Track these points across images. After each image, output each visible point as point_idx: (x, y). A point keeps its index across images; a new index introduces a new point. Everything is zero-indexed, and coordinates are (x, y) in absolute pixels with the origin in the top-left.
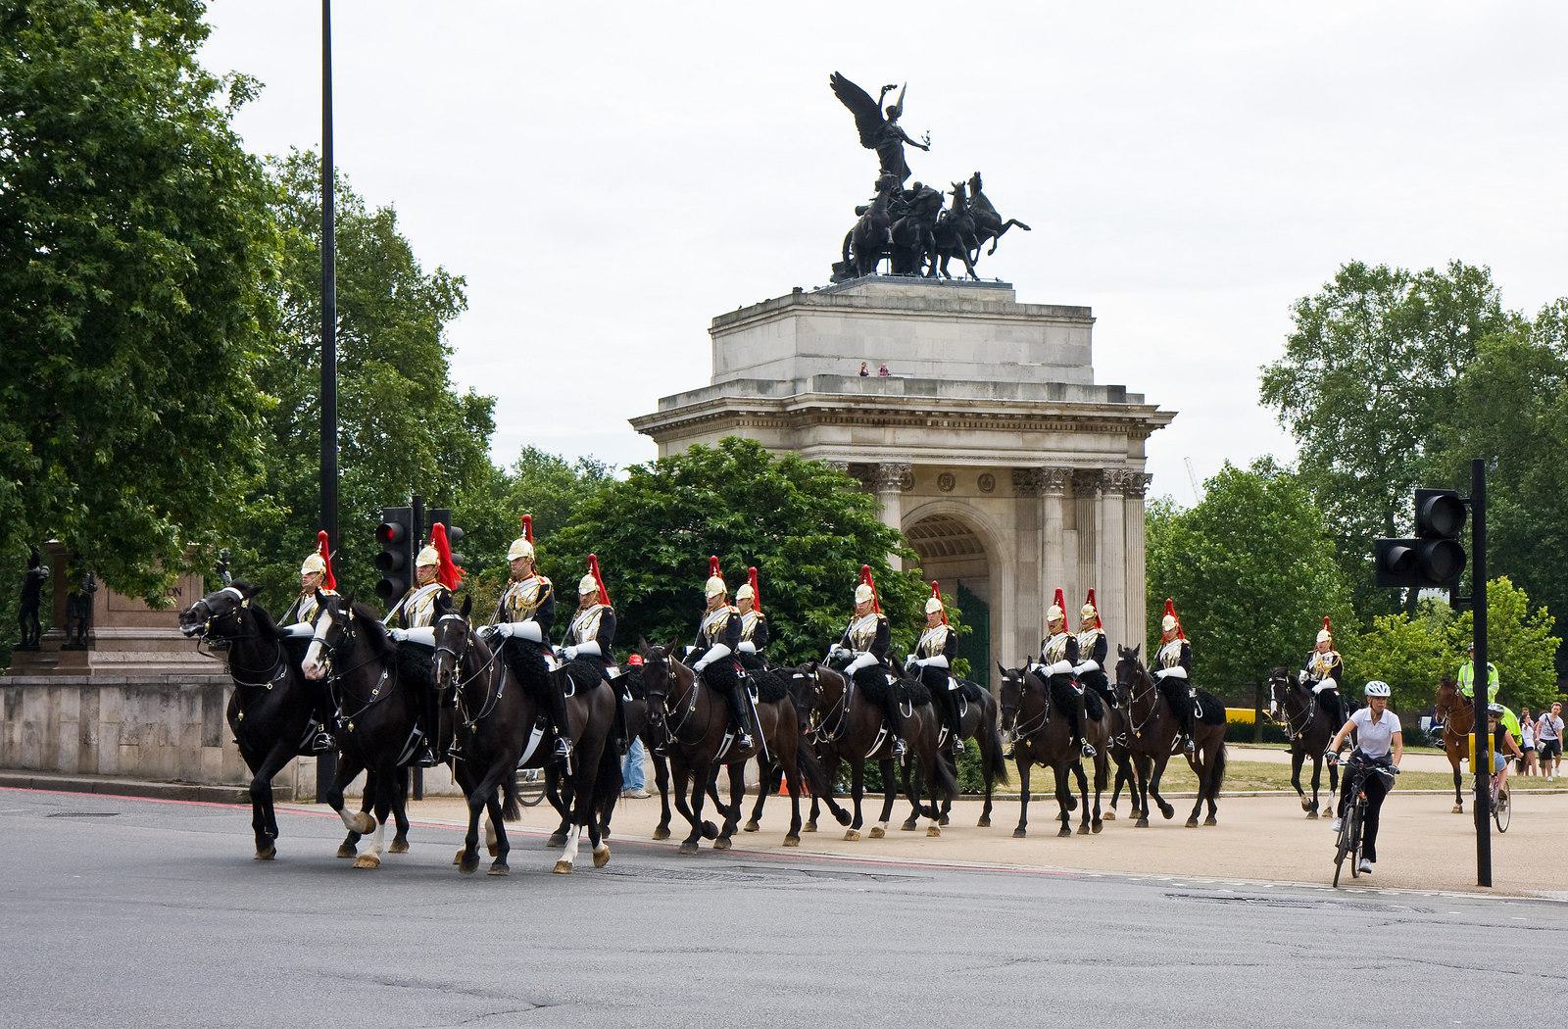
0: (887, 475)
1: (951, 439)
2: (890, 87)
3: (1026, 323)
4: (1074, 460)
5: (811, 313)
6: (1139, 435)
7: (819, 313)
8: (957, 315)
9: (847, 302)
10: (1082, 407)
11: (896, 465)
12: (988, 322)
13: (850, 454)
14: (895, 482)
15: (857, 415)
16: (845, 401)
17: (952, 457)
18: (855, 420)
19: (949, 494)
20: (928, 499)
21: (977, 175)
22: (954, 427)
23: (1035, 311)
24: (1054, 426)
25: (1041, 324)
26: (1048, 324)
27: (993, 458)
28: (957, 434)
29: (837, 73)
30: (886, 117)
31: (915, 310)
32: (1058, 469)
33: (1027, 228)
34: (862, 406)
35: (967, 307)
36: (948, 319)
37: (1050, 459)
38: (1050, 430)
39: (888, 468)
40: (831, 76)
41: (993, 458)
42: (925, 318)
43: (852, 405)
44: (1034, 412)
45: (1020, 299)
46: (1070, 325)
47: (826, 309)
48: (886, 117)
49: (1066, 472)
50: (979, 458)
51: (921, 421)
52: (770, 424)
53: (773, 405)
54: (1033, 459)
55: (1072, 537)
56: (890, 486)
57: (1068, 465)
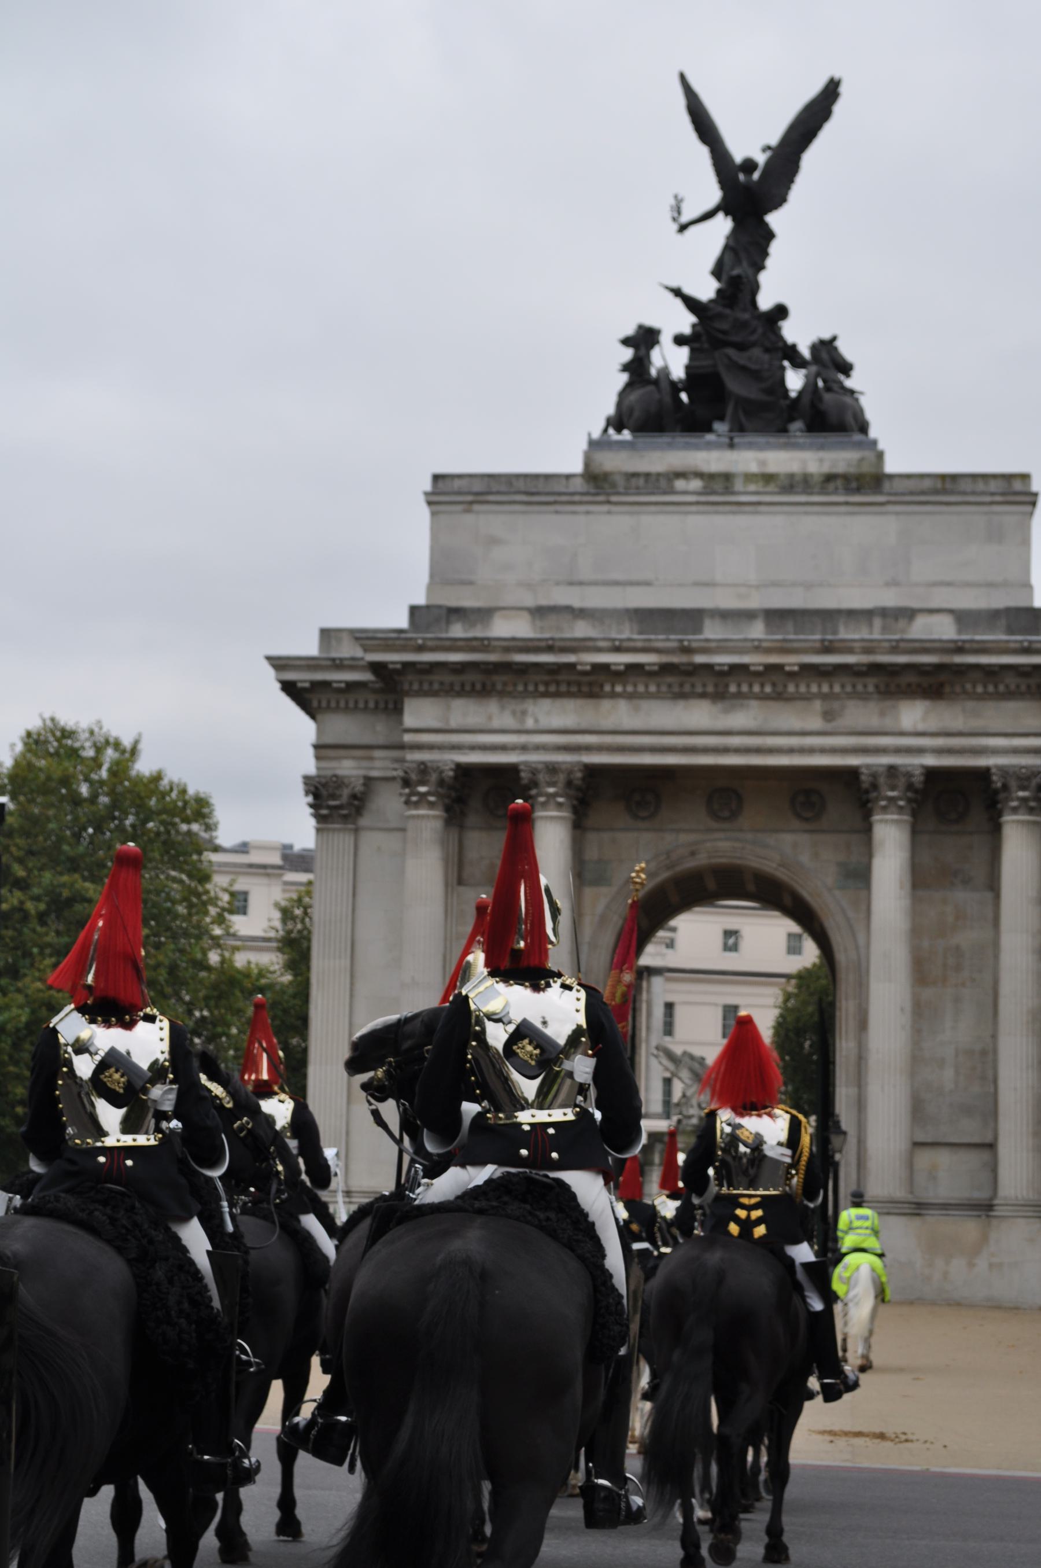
20: (684, 838)
39: (534, 772)
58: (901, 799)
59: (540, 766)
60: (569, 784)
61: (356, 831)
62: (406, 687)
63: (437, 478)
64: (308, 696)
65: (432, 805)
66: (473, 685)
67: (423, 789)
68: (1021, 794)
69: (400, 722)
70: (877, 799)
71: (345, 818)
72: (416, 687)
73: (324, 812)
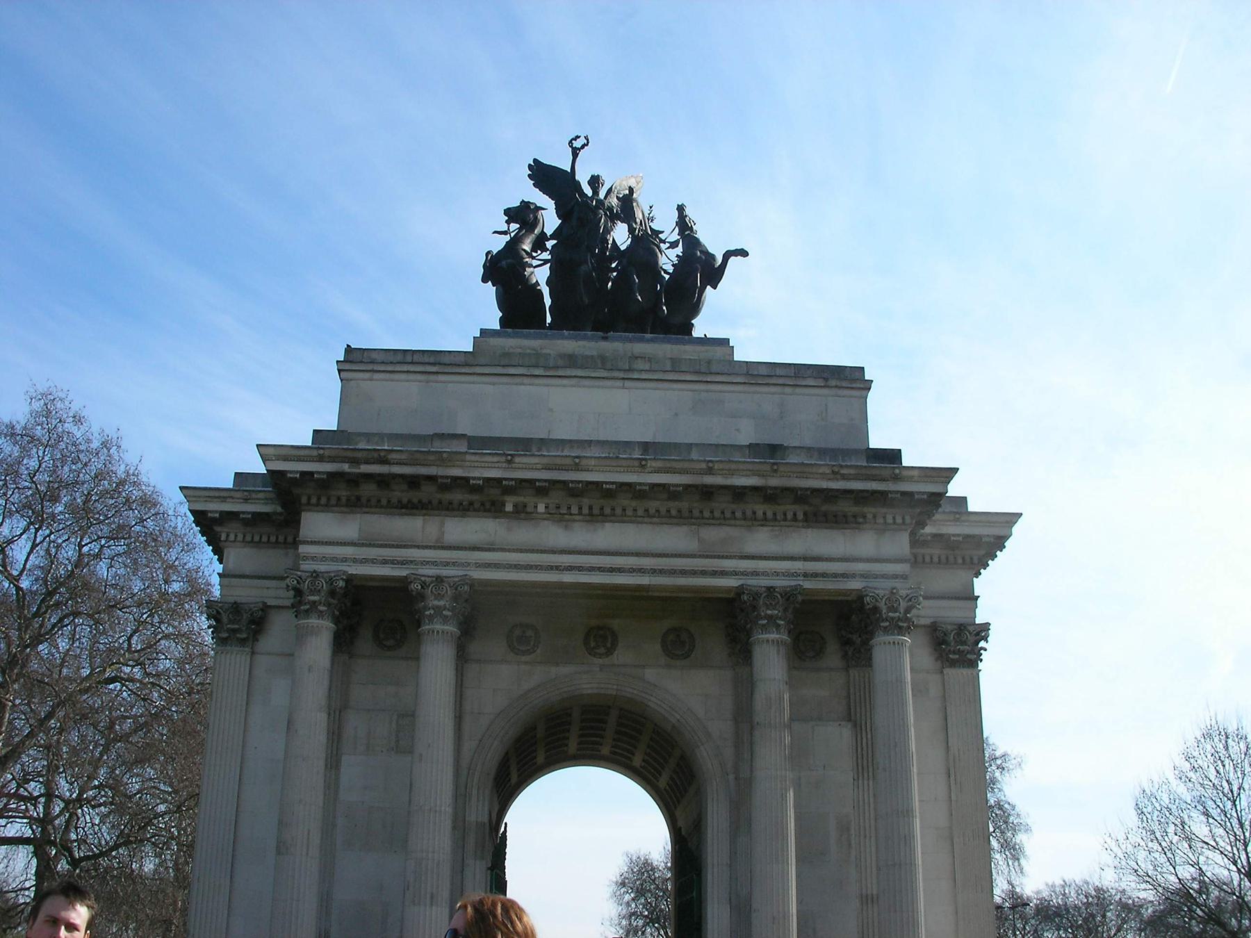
0: (422, 597)
1: (554, 535)
2: (578, 137)
3: (746, 388)
4: (805, 575)
5: (367, 375)
6: (960, 561)
7: (382, 376)
8: (622, 375)
9: (432, 360)
10: (803, 470)
11: (439, 580)
12: (675, 386)
13: (355, 561)
14: (438, 609)
15: (368, 490)
16: (332, 459)
17: (557, 568)
18: (364, 500)
19: (606, 661)
21: (681, 209)
22: (559, 516)
23: (763, 371)
24: (760, 514)
25: (773, 389)
26: (788, 390)
27: (641, 571)
28: (566, 527)
29: (535, 160)
30: (588, 191)
31: (546, 368)
32: (770, 590)
33: (743, 253)
34: (365, 469)
35: (640, 365)
36: (609, 383)
37: (755, 573)
38: (754, 521)
39: (424, 585)
40: (530, 165)
41: (641, 571)
42: (565, 381)
43: (346, 467)
44: (709, 480)
45: (739, 356)
46: (825, 391)
47: (390, 368)
48: (588, 191)
49: (789, 595)
50: (612, 570)
51: (493, 503)
52: (273, 539)
53: (267, 501)
54: (723, 573)
55: (838, 737)
56: (431, 618)
57: (793, 583)
58: (780, 619)
59: (428, 580)
60: (455, 598)
61: (253, 653)
62: (304, 500)
63: (349, 350)
64: (218, 529)
65: (321, 615)
66: (369, 501)
67: (312, 598)
68: (891, 614)
69: (296, 535)
70: (759, 617)
71: (243, 642)
72: (314, 501)
73: (225, 635)
